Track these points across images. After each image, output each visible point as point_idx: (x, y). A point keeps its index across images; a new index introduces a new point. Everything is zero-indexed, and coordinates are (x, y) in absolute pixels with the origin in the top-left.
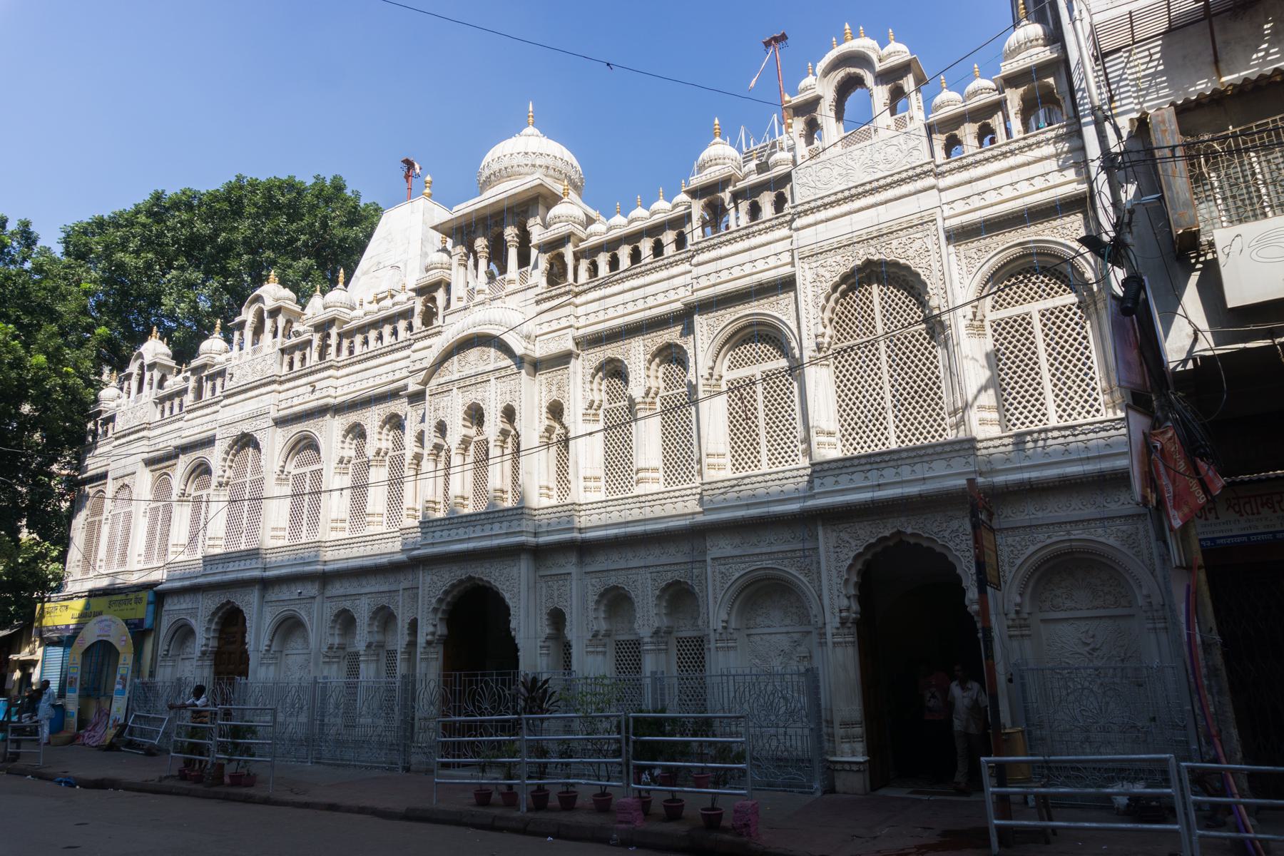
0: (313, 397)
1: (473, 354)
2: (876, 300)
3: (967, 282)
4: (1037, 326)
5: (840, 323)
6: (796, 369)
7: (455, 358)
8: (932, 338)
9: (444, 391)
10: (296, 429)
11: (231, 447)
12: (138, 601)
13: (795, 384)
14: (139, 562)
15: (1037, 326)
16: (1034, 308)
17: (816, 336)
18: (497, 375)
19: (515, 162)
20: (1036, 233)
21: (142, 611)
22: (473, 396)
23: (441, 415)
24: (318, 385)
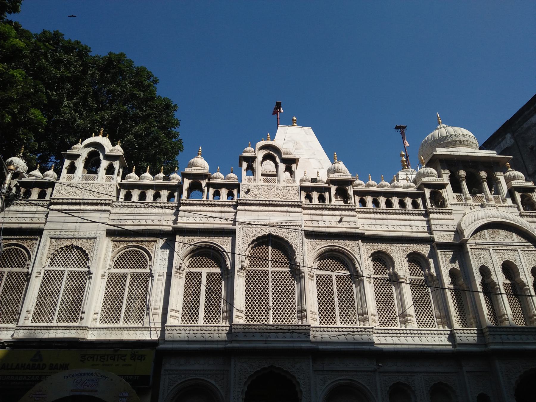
0: (340, 225)
1: (503, 233)
2: (270, 252)
3: (310, 255)
4: (334, 282)
5: (252, 257)
6: (228, 275)
7: (486, 231)
8: (293, 276)
9: (482, 247)
10: (325, 244)
11: (253, 241)
12: (142, 358)
13: (223, 282)
14: (95, 320)
15: (334, 282)
16: (334, 274)
17: (242, 262)
18: (522, 248)
19: (471, 140)
20: (338, 243)
21: (145, 368)
22: (509, 256)
23: (483, 262)
24: (345, 219)
